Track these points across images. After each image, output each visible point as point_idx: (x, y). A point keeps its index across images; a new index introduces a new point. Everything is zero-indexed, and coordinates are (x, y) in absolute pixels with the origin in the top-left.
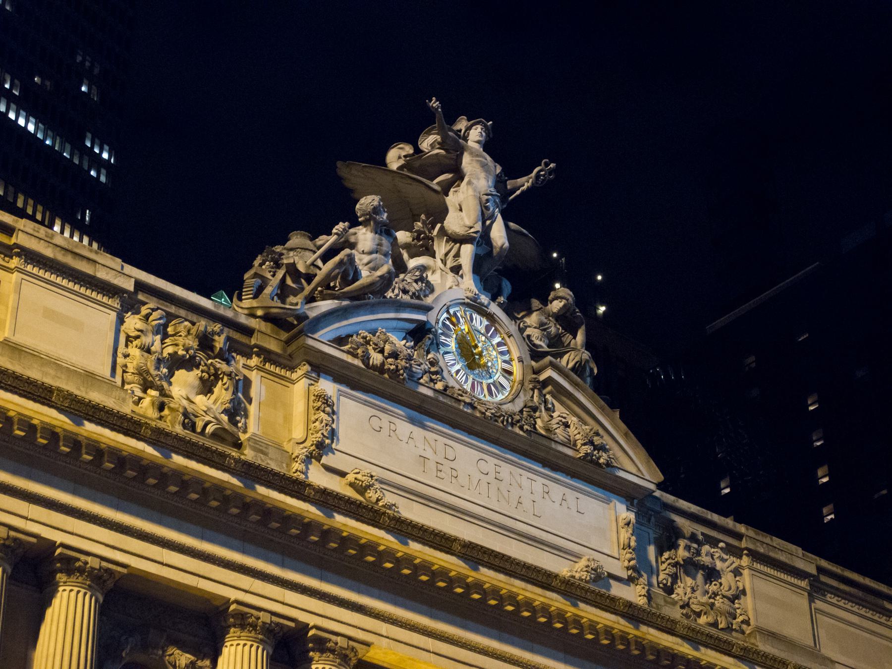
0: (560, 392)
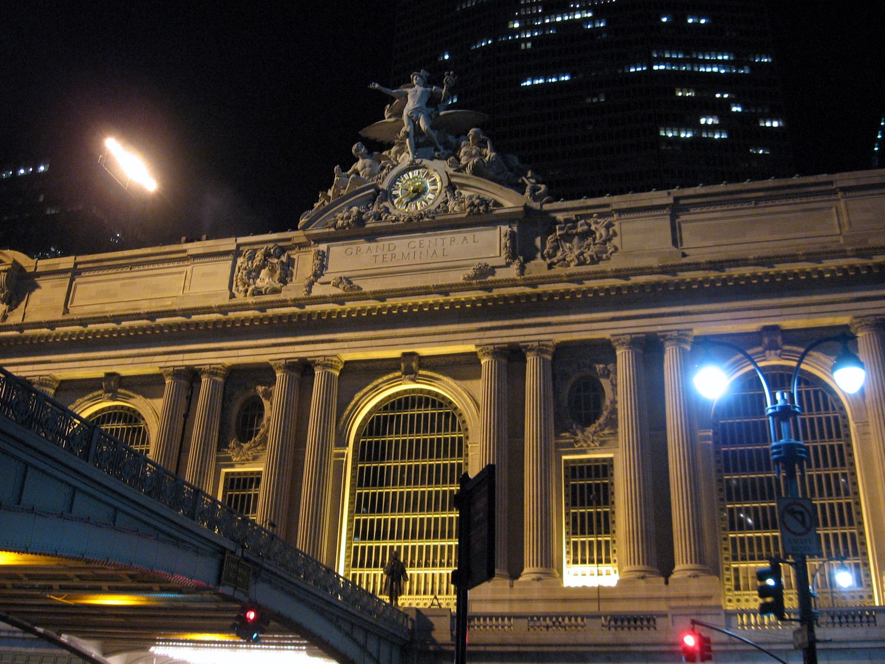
0: (463, 186)
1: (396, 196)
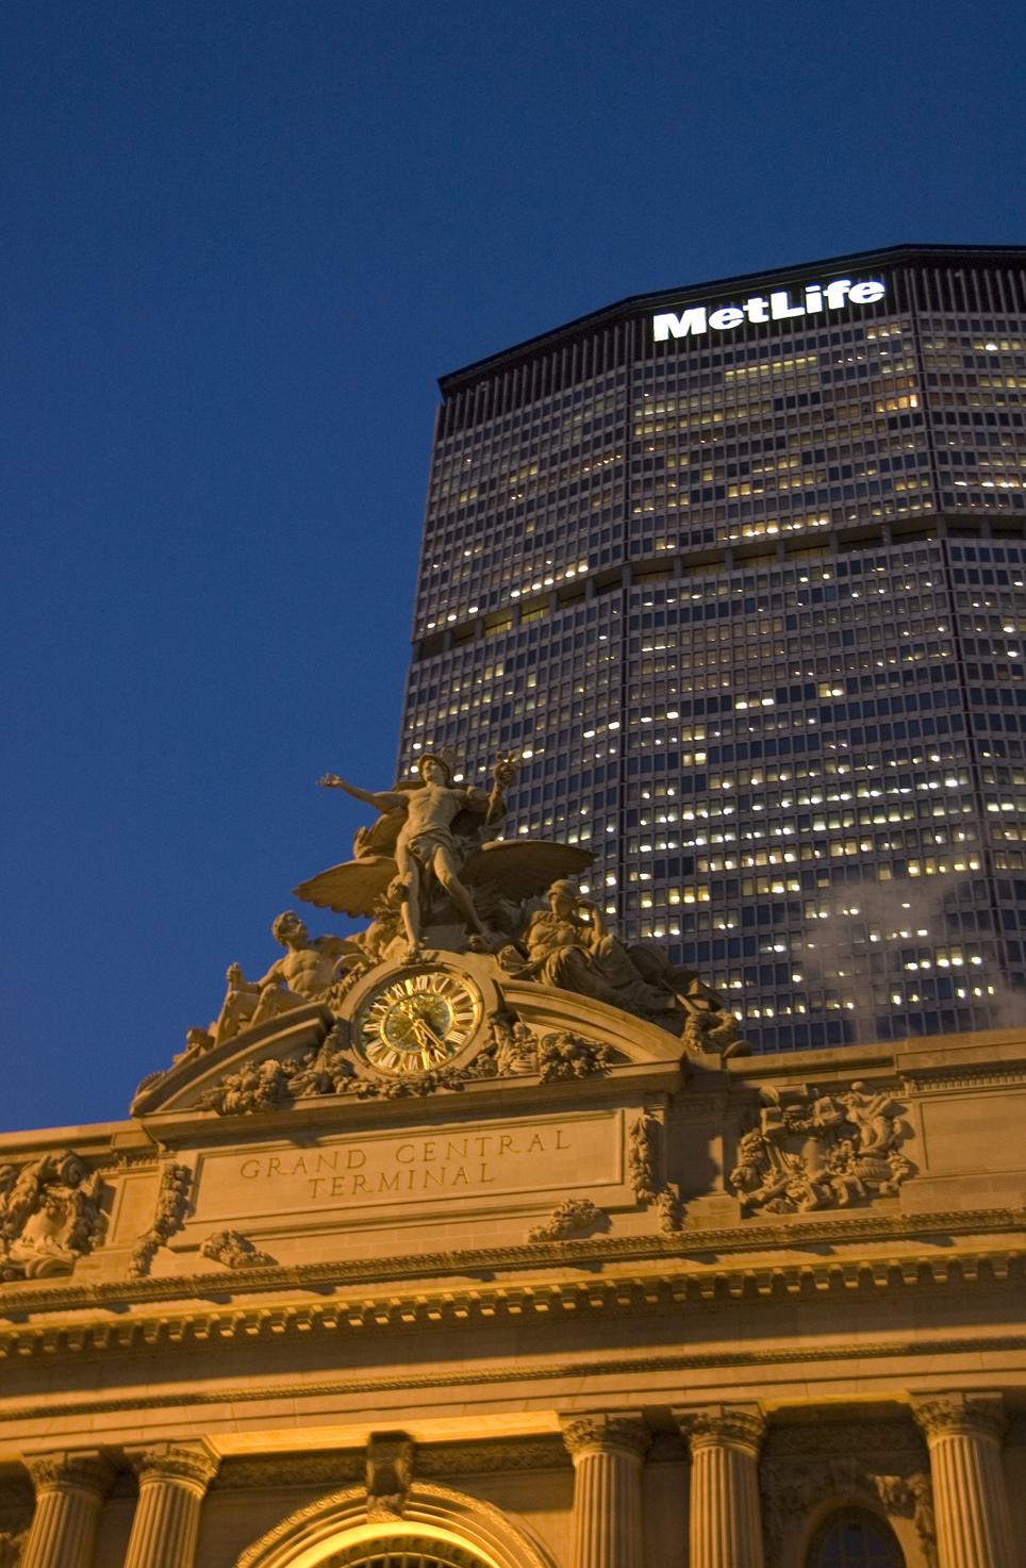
0: (533, 1012)
1: (371, 1037)
